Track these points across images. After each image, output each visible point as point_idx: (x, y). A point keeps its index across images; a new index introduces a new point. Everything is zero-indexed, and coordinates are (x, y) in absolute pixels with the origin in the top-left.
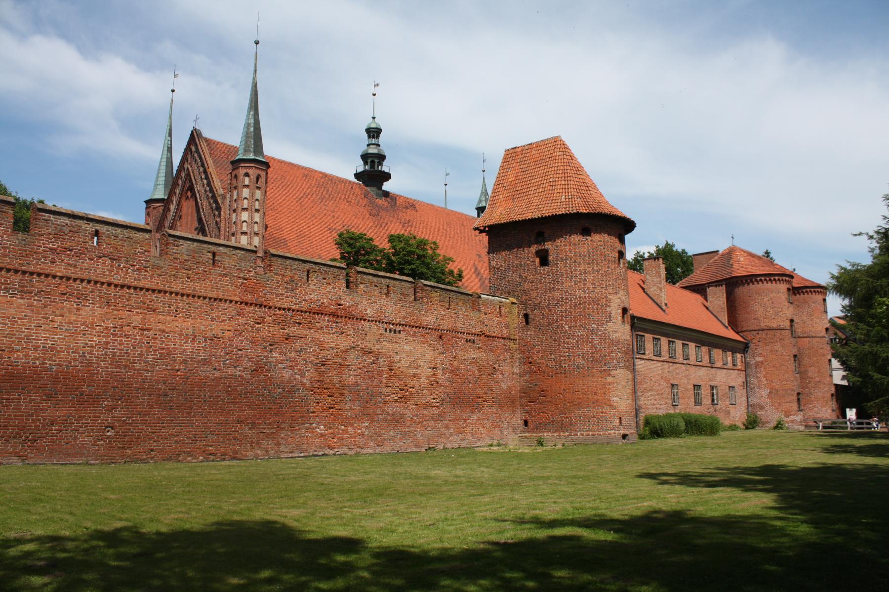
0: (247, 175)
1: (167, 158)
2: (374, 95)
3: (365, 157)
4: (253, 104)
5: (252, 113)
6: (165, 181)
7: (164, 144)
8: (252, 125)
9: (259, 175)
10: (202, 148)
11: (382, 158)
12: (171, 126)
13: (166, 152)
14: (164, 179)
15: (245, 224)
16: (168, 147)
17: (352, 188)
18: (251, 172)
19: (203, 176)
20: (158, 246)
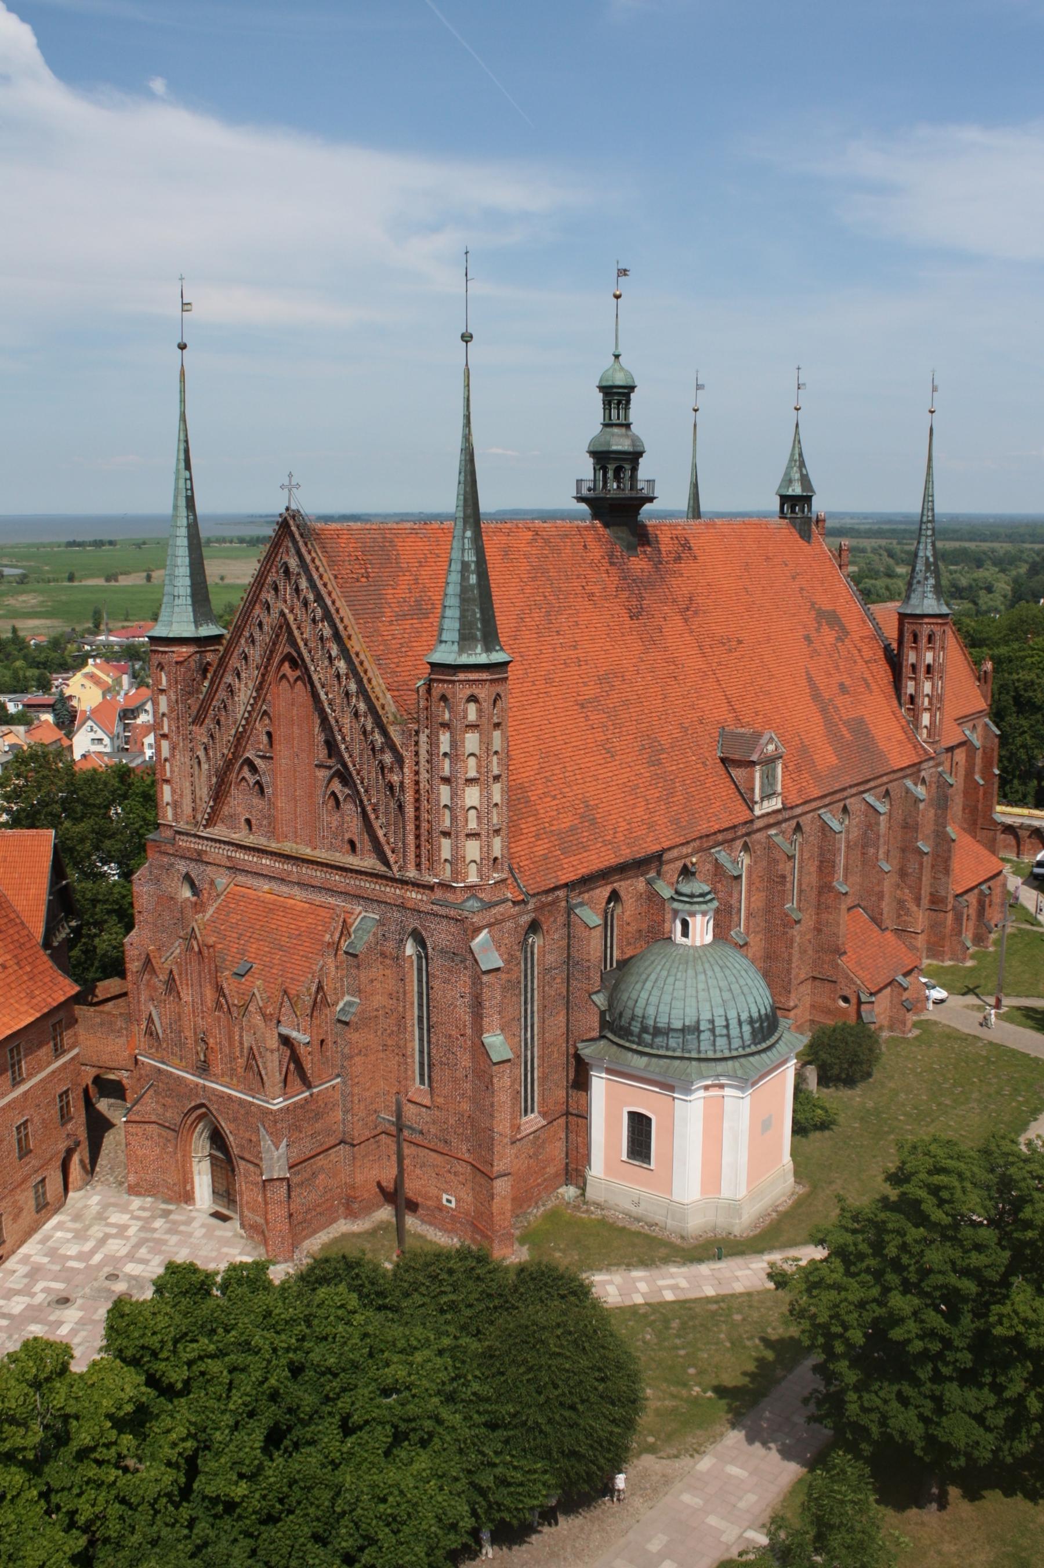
0: (473, 699)
1: (189, 526)
2: (617, 297)
3: (601, 457)
4: (470, 503)
5: (469, 534)
6: (193, 586)
7: (176, 489)
8: (473, 567)
9: (498, 695)
10: (317, 569)
11: (634, 457)
12: (186, 442)
13: (183, 511)
14: (187, 581)
15: (473, 812)
16: (187, 497)
17: (585, 546)
18: (482, 692)
19: (334, 652)
20: (203, 758)
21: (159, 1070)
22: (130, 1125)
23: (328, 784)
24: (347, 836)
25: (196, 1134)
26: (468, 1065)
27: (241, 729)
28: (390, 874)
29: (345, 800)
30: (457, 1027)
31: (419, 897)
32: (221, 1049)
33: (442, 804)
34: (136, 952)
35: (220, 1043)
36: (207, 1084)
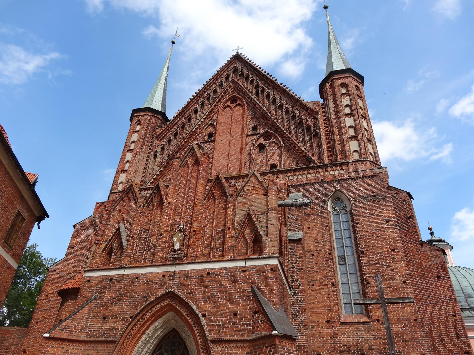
21: (111, 279)
22: (51, 343)
23: (257, 140)
24: (269, 163)
25: (140, 343)
26: (404, 272)
27: (194, 130)
28: (313, 165)
29: (269, 146)
30: (387, 244)
31: (337, 172)
32: (204, 233)
33: (347, 127)
34: (58, 276)
35: (204, 228)
36: (180, 268)
